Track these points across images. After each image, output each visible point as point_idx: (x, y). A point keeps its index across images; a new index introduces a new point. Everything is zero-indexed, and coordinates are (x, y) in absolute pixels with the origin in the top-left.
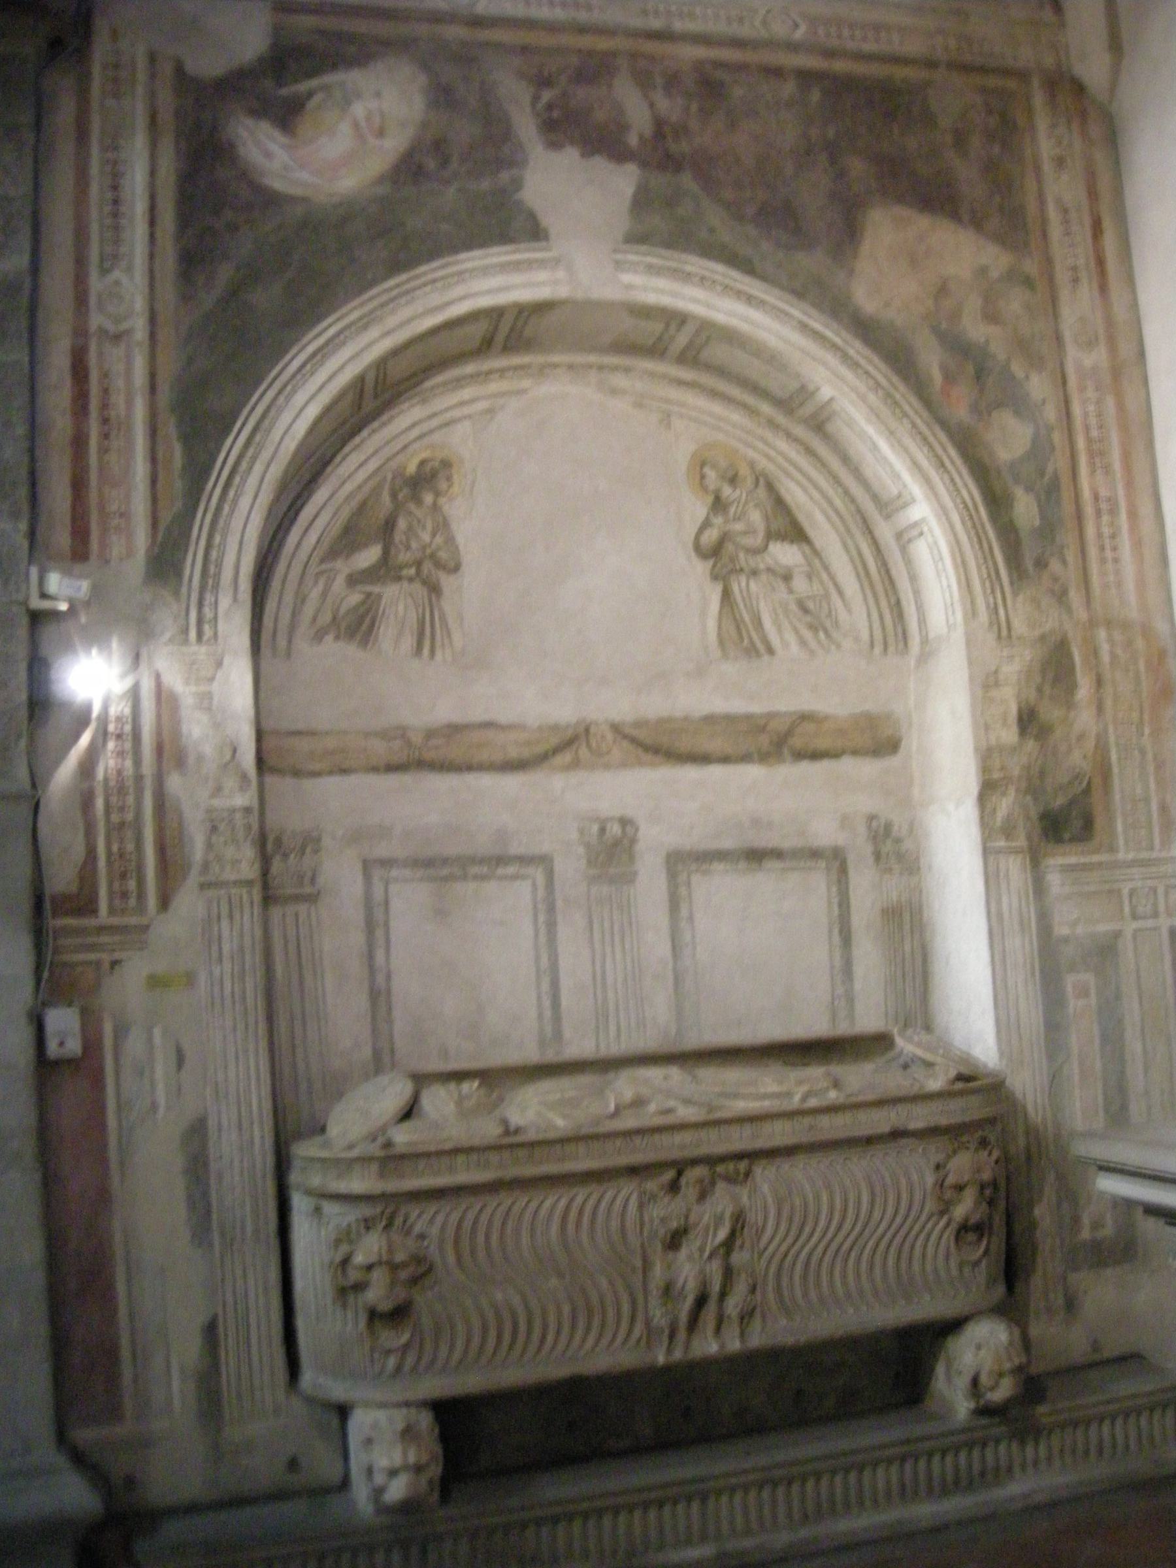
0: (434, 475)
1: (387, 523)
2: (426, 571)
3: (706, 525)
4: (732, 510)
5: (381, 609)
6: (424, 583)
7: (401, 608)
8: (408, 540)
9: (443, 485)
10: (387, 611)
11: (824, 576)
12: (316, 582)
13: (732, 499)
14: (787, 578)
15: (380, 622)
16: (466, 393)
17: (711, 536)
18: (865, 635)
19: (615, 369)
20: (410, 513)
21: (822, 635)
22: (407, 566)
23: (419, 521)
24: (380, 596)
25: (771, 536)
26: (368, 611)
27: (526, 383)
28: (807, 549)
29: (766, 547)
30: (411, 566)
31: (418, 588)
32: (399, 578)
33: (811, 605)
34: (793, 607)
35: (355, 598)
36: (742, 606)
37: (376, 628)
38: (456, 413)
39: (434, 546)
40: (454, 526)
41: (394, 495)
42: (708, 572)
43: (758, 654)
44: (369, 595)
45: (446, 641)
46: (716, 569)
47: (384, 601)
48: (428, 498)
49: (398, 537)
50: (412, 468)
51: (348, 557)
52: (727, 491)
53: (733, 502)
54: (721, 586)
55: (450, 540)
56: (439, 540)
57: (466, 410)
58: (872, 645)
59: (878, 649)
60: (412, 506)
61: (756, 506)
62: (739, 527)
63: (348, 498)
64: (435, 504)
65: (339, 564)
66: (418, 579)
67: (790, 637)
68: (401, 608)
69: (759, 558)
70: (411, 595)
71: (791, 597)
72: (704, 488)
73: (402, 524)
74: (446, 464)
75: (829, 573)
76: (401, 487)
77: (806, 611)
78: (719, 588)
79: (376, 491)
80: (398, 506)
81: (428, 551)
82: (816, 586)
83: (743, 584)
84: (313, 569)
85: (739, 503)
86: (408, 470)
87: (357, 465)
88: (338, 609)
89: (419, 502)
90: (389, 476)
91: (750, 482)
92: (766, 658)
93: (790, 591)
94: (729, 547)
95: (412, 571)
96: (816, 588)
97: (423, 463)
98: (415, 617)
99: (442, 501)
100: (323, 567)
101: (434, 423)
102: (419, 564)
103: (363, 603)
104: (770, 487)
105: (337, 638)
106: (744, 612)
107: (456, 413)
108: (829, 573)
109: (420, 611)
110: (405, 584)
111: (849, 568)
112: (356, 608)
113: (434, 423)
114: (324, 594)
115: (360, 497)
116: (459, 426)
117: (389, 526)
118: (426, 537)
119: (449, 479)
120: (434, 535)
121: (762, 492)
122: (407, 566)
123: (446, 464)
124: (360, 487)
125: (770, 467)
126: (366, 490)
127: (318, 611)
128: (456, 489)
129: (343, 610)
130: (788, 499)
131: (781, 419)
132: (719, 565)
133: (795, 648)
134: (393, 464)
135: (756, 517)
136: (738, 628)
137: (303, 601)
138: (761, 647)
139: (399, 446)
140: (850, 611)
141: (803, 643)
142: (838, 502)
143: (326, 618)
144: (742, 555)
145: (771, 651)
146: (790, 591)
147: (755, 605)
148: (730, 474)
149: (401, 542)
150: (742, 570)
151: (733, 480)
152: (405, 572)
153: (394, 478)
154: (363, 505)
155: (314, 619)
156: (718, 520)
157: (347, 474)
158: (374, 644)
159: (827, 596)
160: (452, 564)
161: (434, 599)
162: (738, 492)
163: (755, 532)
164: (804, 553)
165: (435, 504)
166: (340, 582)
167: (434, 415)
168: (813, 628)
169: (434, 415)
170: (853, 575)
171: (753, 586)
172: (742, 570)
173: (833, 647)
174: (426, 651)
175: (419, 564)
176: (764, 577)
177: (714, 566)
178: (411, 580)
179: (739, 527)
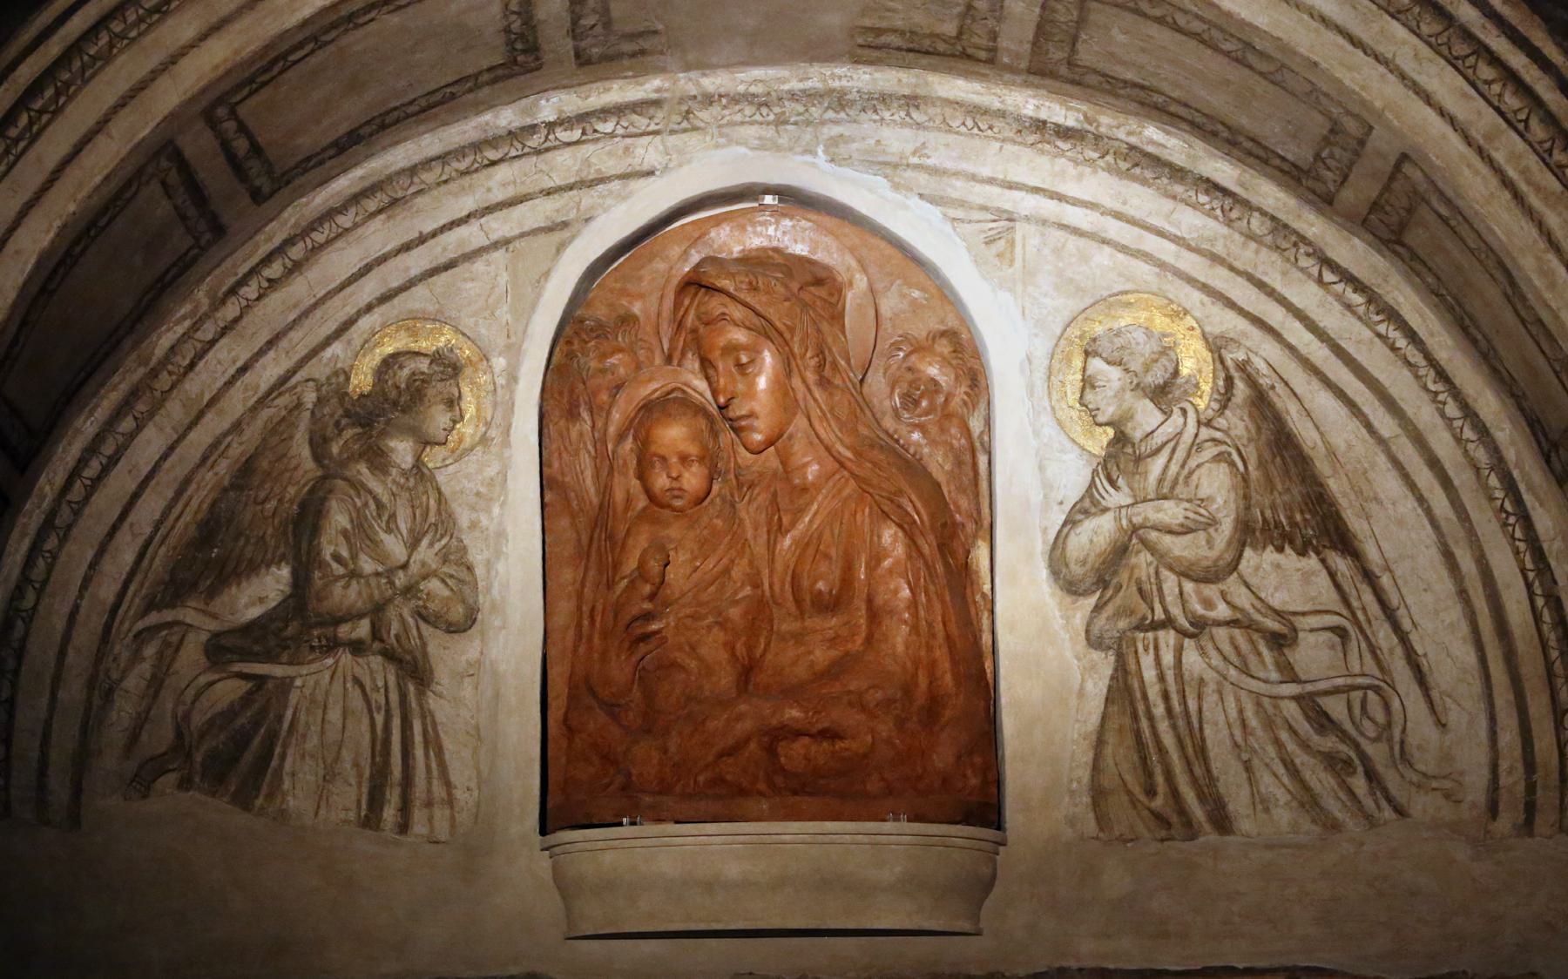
0: (416, 393)
1: (303, 506)
2: (395, 627)
3: (1087, 506)
4: (1156, 466)
5: (289, 714)
6: (389, 655)
7: (334, 715)
8: (354, 557)
9: (439, 418)
10: (303, 717)
11: (1384, 636)
12: (136, 657)
13: (1158, 439)
14: (1281, 641)
15: (285, 746)
16: (500, 181)
17: (1097, 533)
18: (1476, 782)
19: (879, 101)
20: (358, 486)
21: (1359, 783)
22: (353, 616)
23: (380, 506)
24: (285, 685)
25: (1248, 533)
26: (256, 724)
27: (647, 152)
28: (1341, 564)
29: (1234, 566)
30: (360, 616)
31: (376, 669)
32: (332, 646)
33: (1335, 707)
34: (1291, 710)
35: (228, 691)
36: (1159, 710)
37: (274, 763)
38: (472, 236)
39: (414, 568)
40: (464, 518)
41: (319, 445)
42: (1079, 620)
43: (1191, 830)
44: (260, 680)
45: (439, 791)
46: (1101, 621)
47: (294, 697)
48: (402, 450)
49: (330, 545)
50: (362, 380)
51: (212, 593)
52: (1147, 417)
53: (1158, 451)
54: (1112, 658)
55: (456, 557)
56: (426, 553)
57: (499, 225)
58: (1493, 809)
59: (1505, 822)
60: (362, 470)
61: (1218, 458)
62: (1172, 512)
63: (215, 447)
64: (418, 464)
65: (188, 615)
66: (377, 645)
67: (1274, 785)
68: (334, 715)
69: (1211, 591)
70: (358, 682)
71: (1291, 689)
72: (1093, 413)
73: (338, 518)
74: (448, 367)
75: (1396, 627)
76: (337, 424)
77: (1323, 721)
78: (1105, 664)
79: (280, 429)
80: (329, 475)
81: (401, 579)
82: (1359, 661)
83: (1168, 658)
84: (128, 625)
85: (1173, 451)
86: (354, 381)
87: (232, 371)
88: (187, 716)
89: (378, 460)
90: (310, 398)
91: (1204, 402)
92: (1210, 837)
93: (1289, 673)
94: (1142, 561)
95: (363, 629)
96: (1359, 661)
97: (390, 363)
98: (367, 737)
99: (433, 458)
100: (153, 618)
101: (417, 261)
102: (377, 611)
103: (247, 700)
104: (1261, 402)
105: (185, 784)
106: (1163, 726)
107: (472, 236)
108: (1396, 627)
109: (379, 719)
110: (346, 658)
111: (1454, 613)
112: (231, 713)
113: (417, 261)
114: (156, 683)
115: (238, 449)
116: (479, 266)
117: (309, 516)
118: (395, 547)
119: (452, 403)
120: (413, 545)
121: (1237, 423)
122: (353, 616)
123: (448, 367)
124: (237, 427)
125: (1264, 354)
126: (253, 433)
127: (141, 722)
128: (467, 430)
129: (198, 720)
130: (1306, 434)
131: (1313, 225)
132: (1109, 610)
133: (1283, 816)
134: (318, 369)
135: (1216, 485)
136: (1144, 760)
137: (108, 695)
138: (1198, 812)
139: (331, 327)
140: (1442, 725)
141: (1308, 800)
142: (1443, 445)
143: (159, 737)
144: (1170, 582)
145: (1222, 821)
146: (1289, 673)
147: (1192, 705)
148: (1157, 376)
149: (337, 558)
150: (1168, 623)
151: (1163, 393)
152: (344, 631)
153: (320, 401)
154: (247, 469)
155: (134, 737)
156: (1115, 498)
157: (207, 397)
158: (270, 796)
159: (1383, 689)
160: (457, 613)
161: (411, 688)
162: (1177, 418)
163: (1213, 522)
164: (1332, 575)
165: (418, 464)
166: (191, 654)
167: (422, 240)
168: (1331, 761)
169: (422, 240)
170: (1464, 628)
171: (1191, 657)
172: (1168, 623)
173: (1388, 813)
174: (390, 814)
175: (377, 611)
176: (1221, 633)
177: (1098, 608)
178: (357, 647)
179: (1172, 512)
